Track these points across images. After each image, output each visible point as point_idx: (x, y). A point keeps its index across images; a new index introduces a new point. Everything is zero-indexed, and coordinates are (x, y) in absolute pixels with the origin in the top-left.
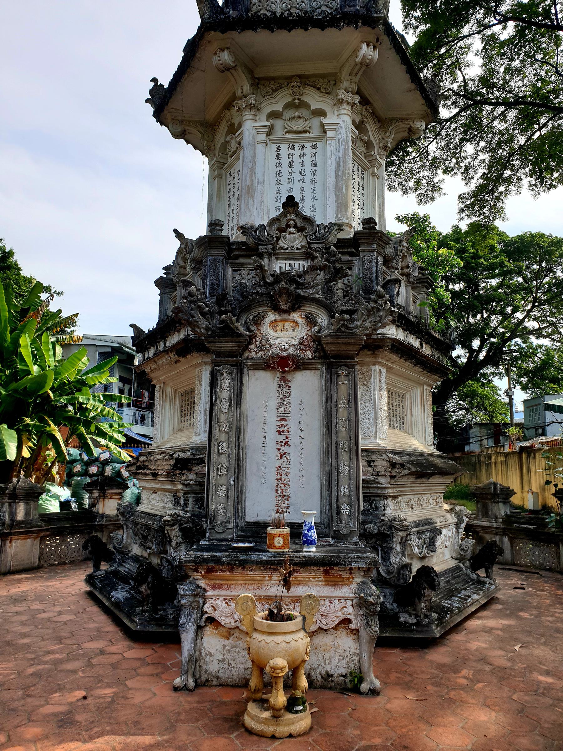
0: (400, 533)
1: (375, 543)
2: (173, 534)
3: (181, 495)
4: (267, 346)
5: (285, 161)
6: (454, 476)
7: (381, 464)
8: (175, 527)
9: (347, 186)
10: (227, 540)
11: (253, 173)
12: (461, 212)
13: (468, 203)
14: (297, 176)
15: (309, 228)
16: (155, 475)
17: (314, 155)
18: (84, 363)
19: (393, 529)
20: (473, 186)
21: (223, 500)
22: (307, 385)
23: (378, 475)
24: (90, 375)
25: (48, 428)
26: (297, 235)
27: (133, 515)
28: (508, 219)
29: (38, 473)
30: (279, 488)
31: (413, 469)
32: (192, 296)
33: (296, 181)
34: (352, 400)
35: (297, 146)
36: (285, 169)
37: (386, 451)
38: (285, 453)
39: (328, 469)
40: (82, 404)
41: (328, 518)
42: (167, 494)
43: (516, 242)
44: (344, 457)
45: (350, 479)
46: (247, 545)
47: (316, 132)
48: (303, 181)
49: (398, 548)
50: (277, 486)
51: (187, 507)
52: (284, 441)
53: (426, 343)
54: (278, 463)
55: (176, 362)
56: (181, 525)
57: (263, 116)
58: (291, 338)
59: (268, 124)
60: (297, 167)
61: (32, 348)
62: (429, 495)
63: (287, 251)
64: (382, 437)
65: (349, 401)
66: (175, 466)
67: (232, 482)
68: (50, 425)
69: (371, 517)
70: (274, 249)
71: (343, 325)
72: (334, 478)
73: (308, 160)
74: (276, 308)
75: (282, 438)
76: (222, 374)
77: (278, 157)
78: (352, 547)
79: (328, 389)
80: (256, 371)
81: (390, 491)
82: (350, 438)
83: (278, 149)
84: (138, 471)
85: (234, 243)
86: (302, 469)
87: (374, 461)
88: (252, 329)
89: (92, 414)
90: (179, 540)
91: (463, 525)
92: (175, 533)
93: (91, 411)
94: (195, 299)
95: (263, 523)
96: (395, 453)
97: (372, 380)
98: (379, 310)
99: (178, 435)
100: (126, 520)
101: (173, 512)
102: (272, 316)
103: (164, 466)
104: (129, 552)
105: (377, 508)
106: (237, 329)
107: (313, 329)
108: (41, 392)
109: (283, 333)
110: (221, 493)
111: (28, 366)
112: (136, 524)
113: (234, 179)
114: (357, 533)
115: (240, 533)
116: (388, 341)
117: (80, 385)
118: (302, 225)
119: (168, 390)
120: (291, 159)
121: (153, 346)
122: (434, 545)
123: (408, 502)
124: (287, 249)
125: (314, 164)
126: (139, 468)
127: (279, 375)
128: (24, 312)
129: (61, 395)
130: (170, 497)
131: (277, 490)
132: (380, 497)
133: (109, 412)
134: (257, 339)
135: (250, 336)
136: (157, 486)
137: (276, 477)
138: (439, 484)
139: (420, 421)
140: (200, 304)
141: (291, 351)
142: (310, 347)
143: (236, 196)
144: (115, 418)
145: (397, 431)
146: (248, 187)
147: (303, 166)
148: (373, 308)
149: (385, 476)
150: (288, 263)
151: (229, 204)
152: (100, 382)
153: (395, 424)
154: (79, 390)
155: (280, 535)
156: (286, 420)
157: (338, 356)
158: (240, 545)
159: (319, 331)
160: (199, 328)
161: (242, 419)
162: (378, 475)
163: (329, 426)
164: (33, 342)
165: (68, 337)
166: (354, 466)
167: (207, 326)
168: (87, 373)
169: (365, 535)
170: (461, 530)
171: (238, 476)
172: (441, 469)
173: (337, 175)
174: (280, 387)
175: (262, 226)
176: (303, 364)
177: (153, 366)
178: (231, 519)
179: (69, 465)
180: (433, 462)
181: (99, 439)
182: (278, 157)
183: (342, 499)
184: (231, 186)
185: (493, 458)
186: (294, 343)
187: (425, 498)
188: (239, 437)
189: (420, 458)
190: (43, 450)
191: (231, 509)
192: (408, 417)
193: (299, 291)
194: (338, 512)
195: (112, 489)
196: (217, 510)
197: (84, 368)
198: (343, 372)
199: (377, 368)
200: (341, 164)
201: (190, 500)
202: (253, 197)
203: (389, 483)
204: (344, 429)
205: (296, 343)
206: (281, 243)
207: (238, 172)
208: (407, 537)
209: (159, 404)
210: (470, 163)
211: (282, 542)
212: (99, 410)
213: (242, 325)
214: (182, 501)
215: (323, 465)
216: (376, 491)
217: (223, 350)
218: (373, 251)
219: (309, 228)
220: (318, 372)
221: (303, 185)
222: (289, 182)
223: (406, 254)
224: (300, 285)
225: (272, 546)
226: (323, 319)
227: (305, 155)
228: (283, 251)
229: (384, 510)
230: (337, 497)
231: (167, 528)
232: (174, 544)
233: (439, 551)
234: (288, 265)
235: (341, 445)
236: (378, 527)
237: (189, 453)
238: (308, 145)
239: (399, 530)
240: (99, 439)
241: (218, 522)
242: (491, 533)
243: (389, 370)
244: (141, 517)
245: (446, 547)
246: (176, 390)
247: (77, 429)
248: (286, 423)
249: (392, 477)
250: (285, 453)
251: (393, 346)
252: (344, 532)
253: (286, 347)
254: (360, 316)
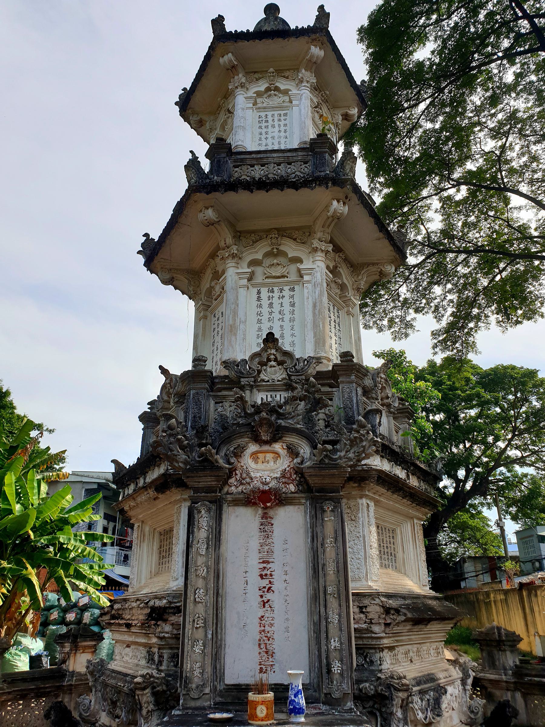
0: (400, 694)
1: (373, 707)
2: (144, 699)
3: (156, 650)
4: (248, 480)
5: (265, 302)
6: (454, 621)
7: (374, 610)
8: (147, 691)
9: (324, 324)
10: (204, 708)
11: (235, 313)
12: (435, 346)
13: (441, 338)
15: (289, 361)
16: (128, 626)
17: (292, 297)
18: (68, 501)
19: (392, 689)
20: (444, 323)
21: (199, 658)
22: (291, 521)
23: (371, 623)
24: (73, 513)
25: (24, 572)
26: (277, 368)
27: (103, 674)
28: (480, 353)
29: (10, 623)
30: (262, 642)
31: (409, 615)
32: (172, 430)
33: (276, 320)
34: (340, 539)
35: (276, 289)
36: (265, 310)
37: (378, 594)
38: (268, 601)
39: (316, 618)
40: (62, 544)
41: (318, 677)
42: (141, 648)
43: (490, 374)
44: (333, 603)
45: (341, 630)
46: (225, 715)
47: (293, 277)
48: (282, 320)
49: (399, 714)
50: (260, 640)
51: (161, 665)
52: (267, 587)
53: (413, 474)
54: (260, 613)
55: (155, 499)
56: (154, 688)
58: (272, 471)
59: (249, 270)
60: (276, 308)
61: (16, 486)
62: (428, 644)
63: (268, 383)
64: (374, 578)
65: (336, 539)
66: (150, 615)
67: (210, 636)
68: (27, 569)
69: (366, 674)
70: (255, 381)
71: (326, 456)
72: (323, 629)
73: (286, 301)
74: (257, 440)
75: (265, 583)
76: (200, 512)
77: (259, 299)
78: (347, 716)
79: (313, 526)
80: (236, 508)
81: (385, 641)
82: (339, 581)
83: (259, 292)
84: (112, 621)
85: (216, 377)
86: (287, 619)
87: (366, 607)
88: (232, 461)
89: (72, 555)
90: (151, 707)
91: (470, 681)
92: (146, 698)
93: (71, 551)
94: (174, 432)
95: (245, 685)
96: (389, 596)
97: (360, 515)
98: (362, 441)
99: (155, 579)
100: (96, 681)
101: (145, 672)
102: (253, 448)
103: (138, 616)
104: (97, 721)
105: (372, 662)
106: (217, 462)
107: (295, 461)
108: (21, 533)
109: (264, 466)
110: (198, 649)
111: (10, 505)
112: (105, 685)
113: (218, 319)
114: (351, 696)
115: (218, 699)
116: (374, 472)
117: (63, 523)
118: (282, 358)
119: (147, 529)
120: (271, 301)
121: (133, 482)
122: (440, 708)
123: (406, 653)
124: (268, 381)
125: (293, 305)
126: (113, 617)
127: (260, 511)
128: (12, 450)
129: (42, 535)
130: (143, 651)
131: (260, 645)
132: (375, 648)
133: (89, 553)
134: (237, 472)
135: (229, 469)
136: (131, 639)
137: (259, 629)
138: (438, 631)
139: (412, 558)
140: (180, 437)
141: (273, 484)
142: (293, 480)
143: (220, 334)
144: (96, 559)
145: (390, 571)
146: (231, 326)
147: (282, 306)
148: (355, 437)
149: (379, 623)
150: (269, 394)
151: (214, 342)
152: (82, 520)
153: (387, 562)
154: (61, 529)
155: (263, 703)
156: (268, 562)
157: (321, 490)
158: (218, 716)
159: (302, 462)
160: (177, 462)
161: (221, 562)
162: (371, 623)
163: (316, 569)
164: (18, 480)
165: (54, 474)
166: (344, 614)
167: (185, 459)
168: (70, 511)
169: (360, 698)
170: (469, 687)
171: (216, 629)
172: (439, 613)
173: (314, 314)
174: (262, 525)
175: (244, 361)
176: (286, 499)
177: (132, 504)
178: (208, 681)
179: (45, 613)
180: (429, 605)
181: (77, 583)
182: (259, 299)
183: (333, 655)
184: (216, 326)
185: (492, 595)
186: (276, 475)
187: (425, 648)
188: (218, 582)
189: (415, 601)
190: (18, 597)
191: (209, 669)
192: (400, 555)
193: (279, 421)
194: (329, 671)
195: (85, 641)
196: (192, 670)
197: (67, 506)
198: (328, 507)
199: (364, 501)
200: (318, 304)
201: (166, 656)
202: (235, 335)
203: (384, 632)
204: (332, 572)
205: (278, 476)
206: (262, 376)
207: (222, 313)
208: (408, 698)
209: (137, 545)
210: (439, 303)
211: (265, 712)
212: (80, 551)
213: (222, 457)
214: (156, 658)
215: (311, 613)
216: (370, 642)
217: (201, 485)
218: (352, 382)
219: (289, 361)
220: (302, 508)
221: (282, 323)
222: (269, 321)
223: (384, 385)
224: (280, 416)
225: (254, 717)
226: (305, 450)
227: (283, 297)
228: (264, 383)
229: (381, 665)
230: (328, 651)
231: (138, 692)
232: (144, 712)
233: (445, 714)
234: (269, 396)
235: (330, 590)
236: (375, 687)
237: (165, 601)
238: (286, 288)
239: (399, 690)
240: (77, 583)
241: (194, 686)
242: (501, 689)
243: (377, 503)
244: (112, 677)
245: (453, 709)
246: (155, 529)
247: (56, 572)
248: (268, 566)
249: (387, 625)
250: (268, 601)
251: (379, 478)
252: (336, 695)
253: (268, 480)
254: (343, 446)
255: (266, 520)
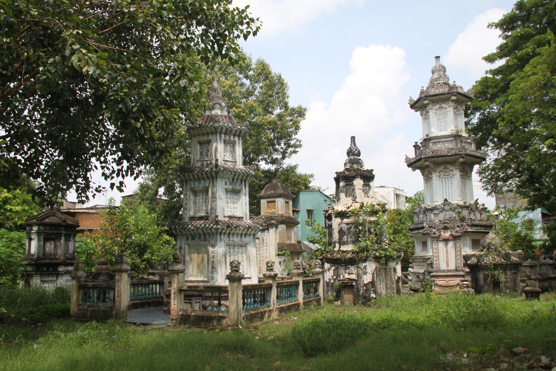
5: (444, 183)
14: (447, 187)
36: (444, 185)
47: (451, 175)
57: (437, 172)
60: (447, 184)
73: (450, 182)
255: (446, 245)
